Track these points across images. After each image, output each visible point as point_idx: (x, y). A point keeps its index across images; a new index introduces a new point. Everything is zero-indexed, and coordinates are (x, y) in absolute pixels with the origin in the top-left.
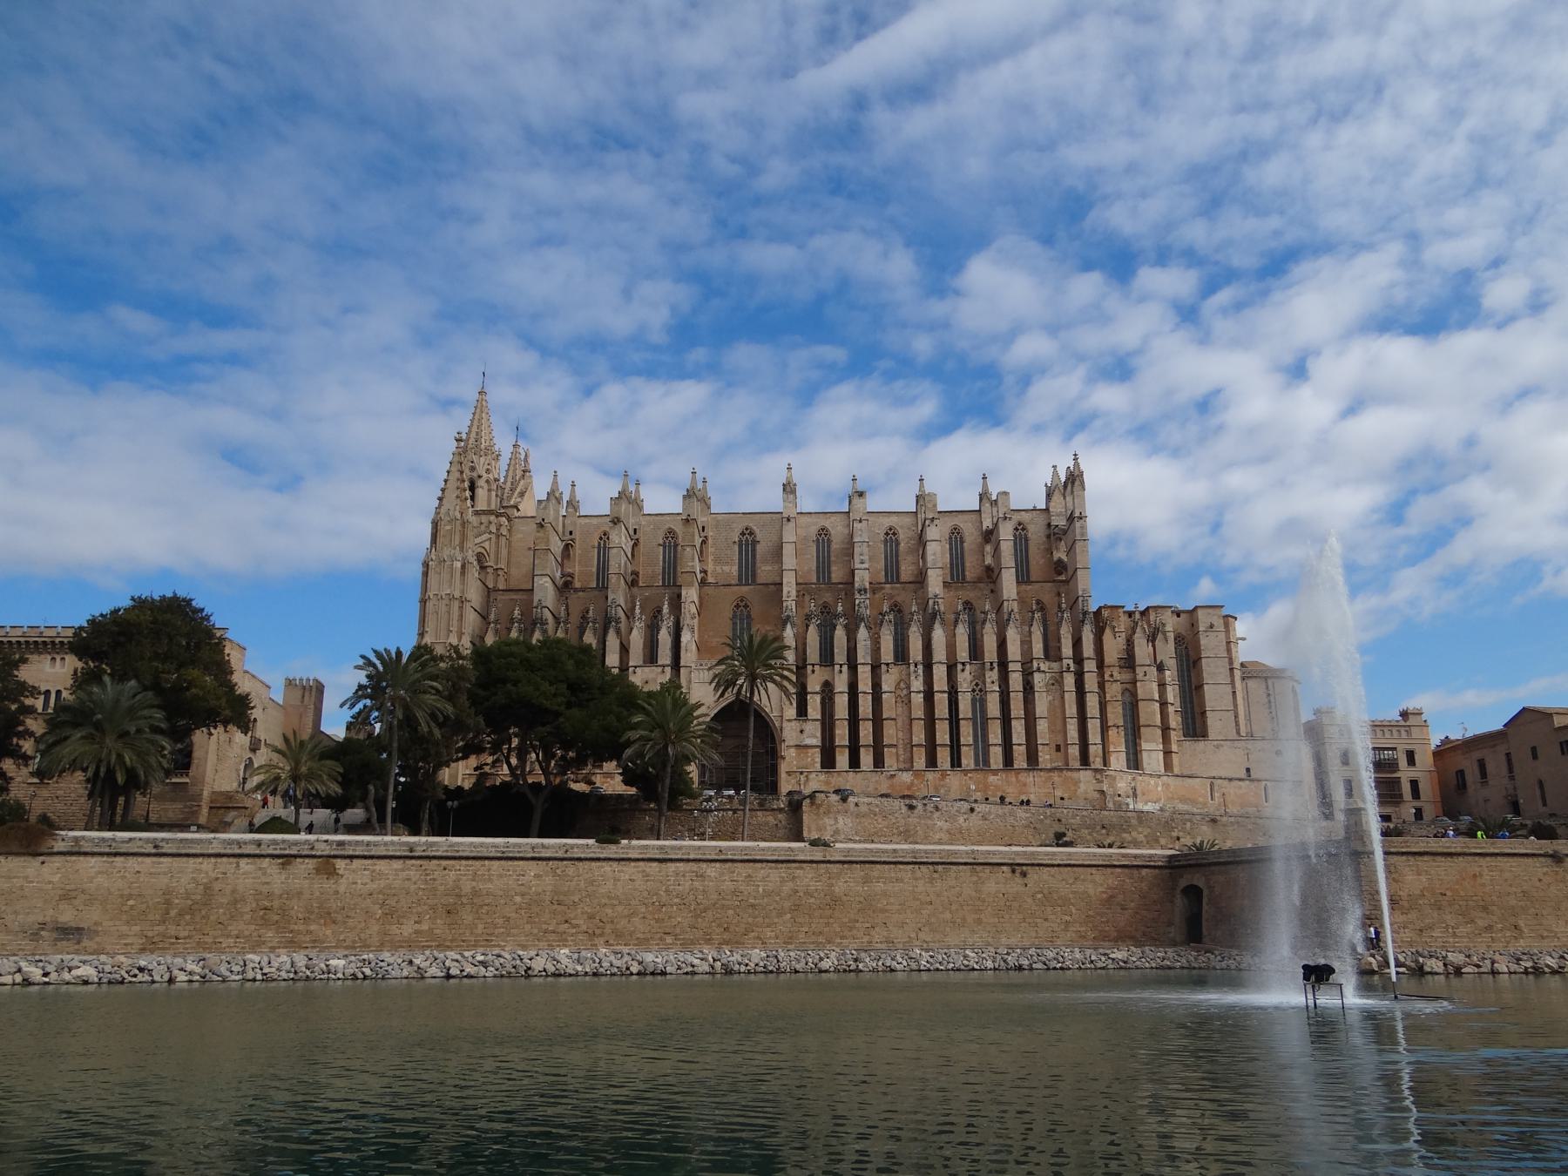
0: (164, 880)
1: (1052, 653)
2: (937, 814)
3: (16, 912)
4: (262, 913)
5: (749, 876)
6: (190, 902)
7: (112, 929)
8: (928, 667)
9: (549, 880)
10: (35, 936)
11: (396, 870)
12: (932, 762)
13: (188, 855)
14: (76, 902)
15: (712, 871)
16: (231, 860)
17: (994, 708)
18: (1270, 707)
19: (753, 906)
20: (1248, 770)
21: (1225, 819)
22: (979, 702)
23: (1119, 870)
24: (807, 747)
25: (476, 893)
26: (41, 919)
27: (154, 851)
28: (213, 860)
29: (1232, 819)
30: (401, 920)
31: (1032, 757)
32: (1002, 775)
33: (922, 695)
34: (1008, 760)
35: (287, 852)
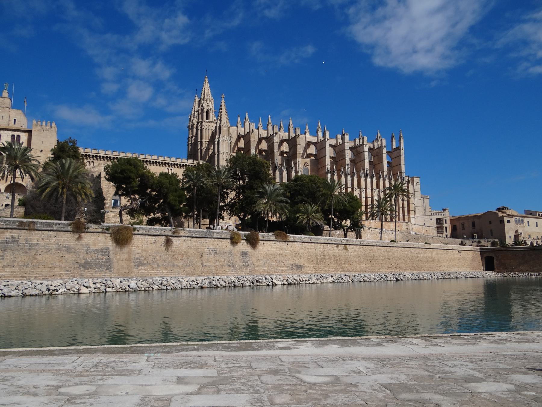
0: (314, 251)
2: (386, 234)
3: (286, 261)
4: (336, 261)
6: (321, 258)
7: (307, 266)
9: (386, 252)
10: (292, 268)
11: (358, 249)
13: (317, 243)
14: (298, 257)
15: (412, 250)
16: (326, 245)
23: (473, 252)
25: (374, 256)
26: (292, 263)
27: (311, 242)
28: (323, 245)
30: (363, 264)
33: (364, 198)
35: (337, 243)
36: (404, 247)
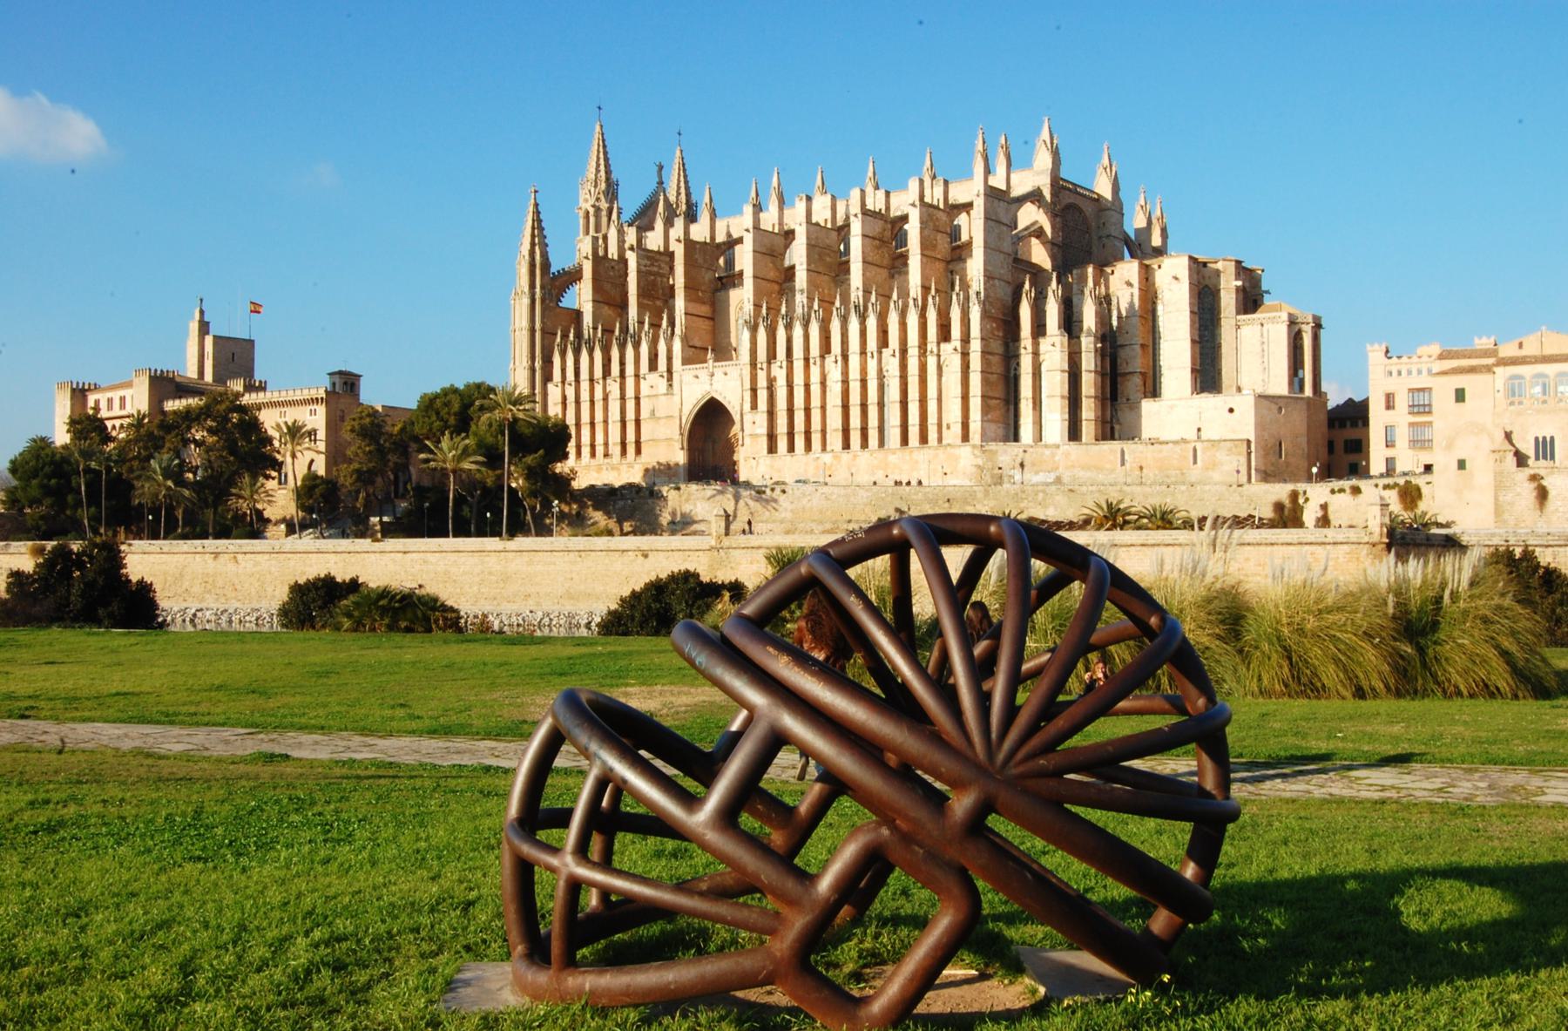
1: (945, 335)
5: (455, 561)
8: (845, 357)
12: (846, 445)
15: (431, 557)
17: (893, 393)
18: (1263, 356)
19: (455, 581)
20: (1199, 430)
21: (1084, 489)
22: (881, 388)
24: (757, 435)
29: (1094, 488)
31: (924, 439)
32: (899, 454)
34: (905, 440)
36: (405, 553)
